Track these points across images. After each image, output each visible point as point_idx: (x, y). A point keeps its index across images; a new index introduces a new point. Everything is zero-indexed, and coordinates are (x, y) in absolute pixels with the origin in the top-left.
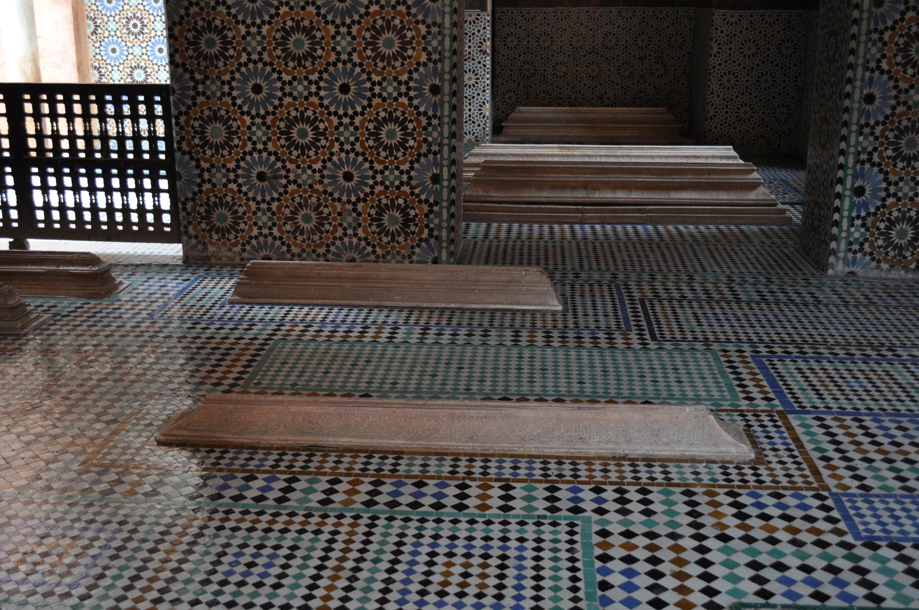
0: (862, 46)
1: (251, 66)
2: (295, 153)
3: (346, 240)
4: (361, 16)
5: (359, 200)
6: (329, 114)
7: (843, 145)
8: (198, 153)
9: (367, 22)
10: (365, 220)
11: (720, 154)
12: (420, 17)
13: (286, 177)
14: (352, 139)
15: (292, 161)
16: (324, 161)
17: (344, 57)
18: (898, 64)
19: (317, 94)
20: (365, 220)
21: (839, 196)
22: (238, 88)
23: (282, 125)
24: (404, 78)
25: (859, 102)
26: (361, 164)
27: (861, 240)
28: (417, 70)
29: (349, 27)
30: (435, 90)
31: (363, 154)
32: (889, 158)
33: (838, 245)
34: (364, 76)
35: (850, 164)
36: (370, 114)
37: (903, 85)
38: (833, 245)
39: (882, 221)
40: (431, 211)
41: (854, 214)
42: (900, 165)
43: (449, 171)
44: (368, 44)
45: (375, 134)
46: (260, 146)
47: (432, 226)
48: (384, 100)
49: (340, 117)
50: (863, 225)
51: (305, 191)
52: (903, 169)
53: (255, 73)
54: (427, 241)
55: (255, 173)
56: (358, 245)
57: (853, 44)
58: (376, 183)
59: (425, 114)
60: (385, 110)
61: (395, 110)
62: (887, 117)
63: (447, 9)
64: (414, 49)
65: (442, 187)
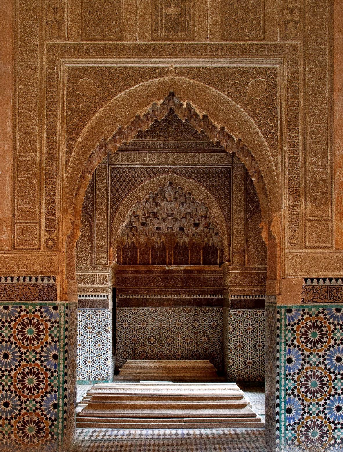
0: (283, 333)
3: (4, 441)
4: (16, 318)
5: (12, 418)
7: (278, 386)
9: (19, 320)
10: (15, 429)
12: (48, 318)
14: (9, 384)
17: (6, 339)
18: (303, 342)
20: (15, 429)
21: (278, 413)
25: (284, 362)
26: (14, 398)
27: (293, 438)
28: (45, 346)
29: (9, 323)
30: (55, 357)
31: (15, 392)
32: (303, 392)
33: (280, 441)
35: (283, 396)
36: (20, 370)
38: (278, 441)
39: (303, 427)
40: (53, 425)
41: (287, 423)
42: (309, 396)
43: (63, 402)
44: (19, 332)
45: (22, 381)
47: (53, 433)
48: (28, 362)
50: (293, 429)
52: (311, 398)
54: (50, 441)
56: (11, 444)
57: (278, 332)
58: (22, 408)
59: (50, 370)
60: (28, 368)
61: (33, 368)
62: (300, 370)
63: (62, 314)
64: (44, 335)
65: (59, 411)
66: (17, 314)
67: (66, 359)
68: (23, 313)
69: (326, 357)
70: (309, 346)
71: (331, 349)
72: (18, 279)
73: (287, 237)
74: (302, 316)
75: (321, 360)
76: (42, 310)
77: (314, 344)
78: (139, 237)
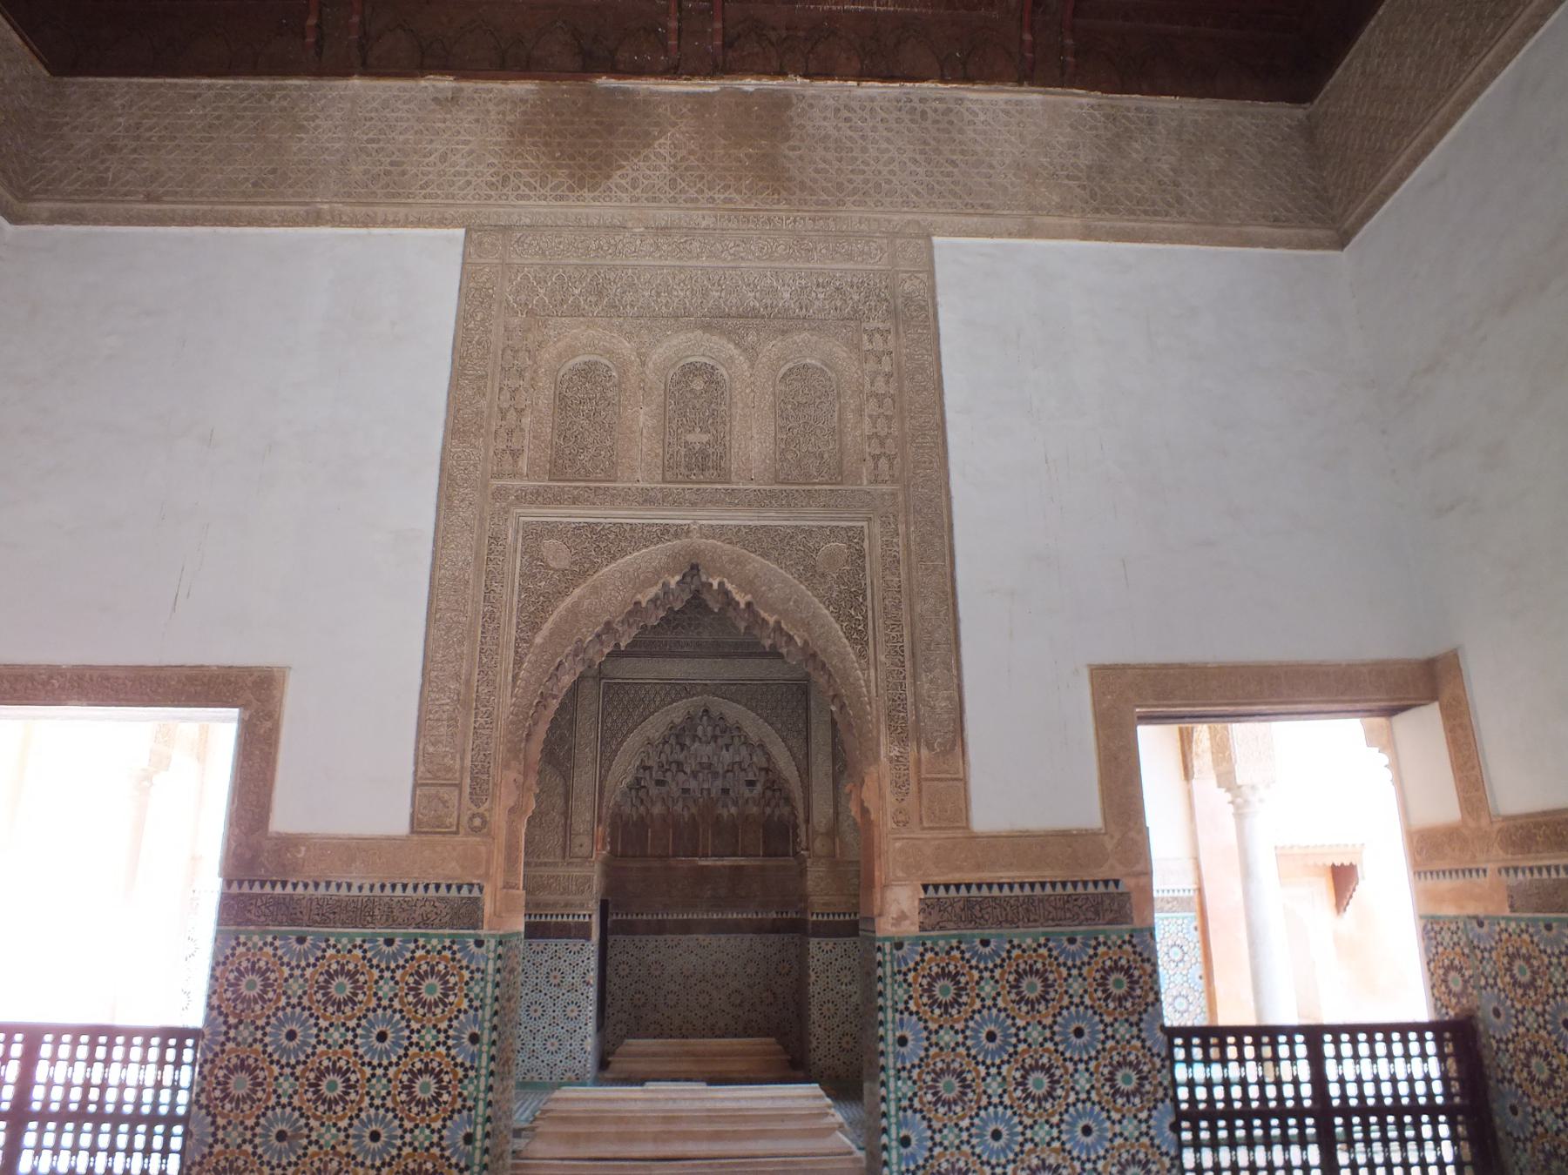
0: (889, 988)
1: (289, 1010)
2: (321, 1108)
6: (363, 1064)
7: (883, 1091)
8: (216, 1107)
11: (803, 1096)
12: (464, 963)
13: (308, 1137)
15: (316, 1118)
16: (351, 1118)
17: (385, 1002)
19: (352, 1042)
21: (885, 1148)
22: (271, 1034)
23: (312, 1076)
24: (444, 1025)
29: (393, 971)
30: (474, 1039)
34: (404, 1023)
35: (893, 1112)
36: (406, 1064)
37: (933, 1026)
44: (411, 989)
45: (408, 1088)
46: (284, 1100)
48: (421, 1049)
49: (374, 1068)
51: (326, 1154)
53: (292, 1018)
55: (275, 1131)
57: (880, 986)
59: (462, 1065)
63: (492, 955)
66: (408, 955)
67: (494, 1043)
68: (419, 953)
69: (968, 1033)
70: (937, 1011)
71: (977, 1016)
72: (415, 887)
73: (890, 810)
74: (922, 955)
75: (960, 1038)
76: (455, 947)
77: (946, 1007)
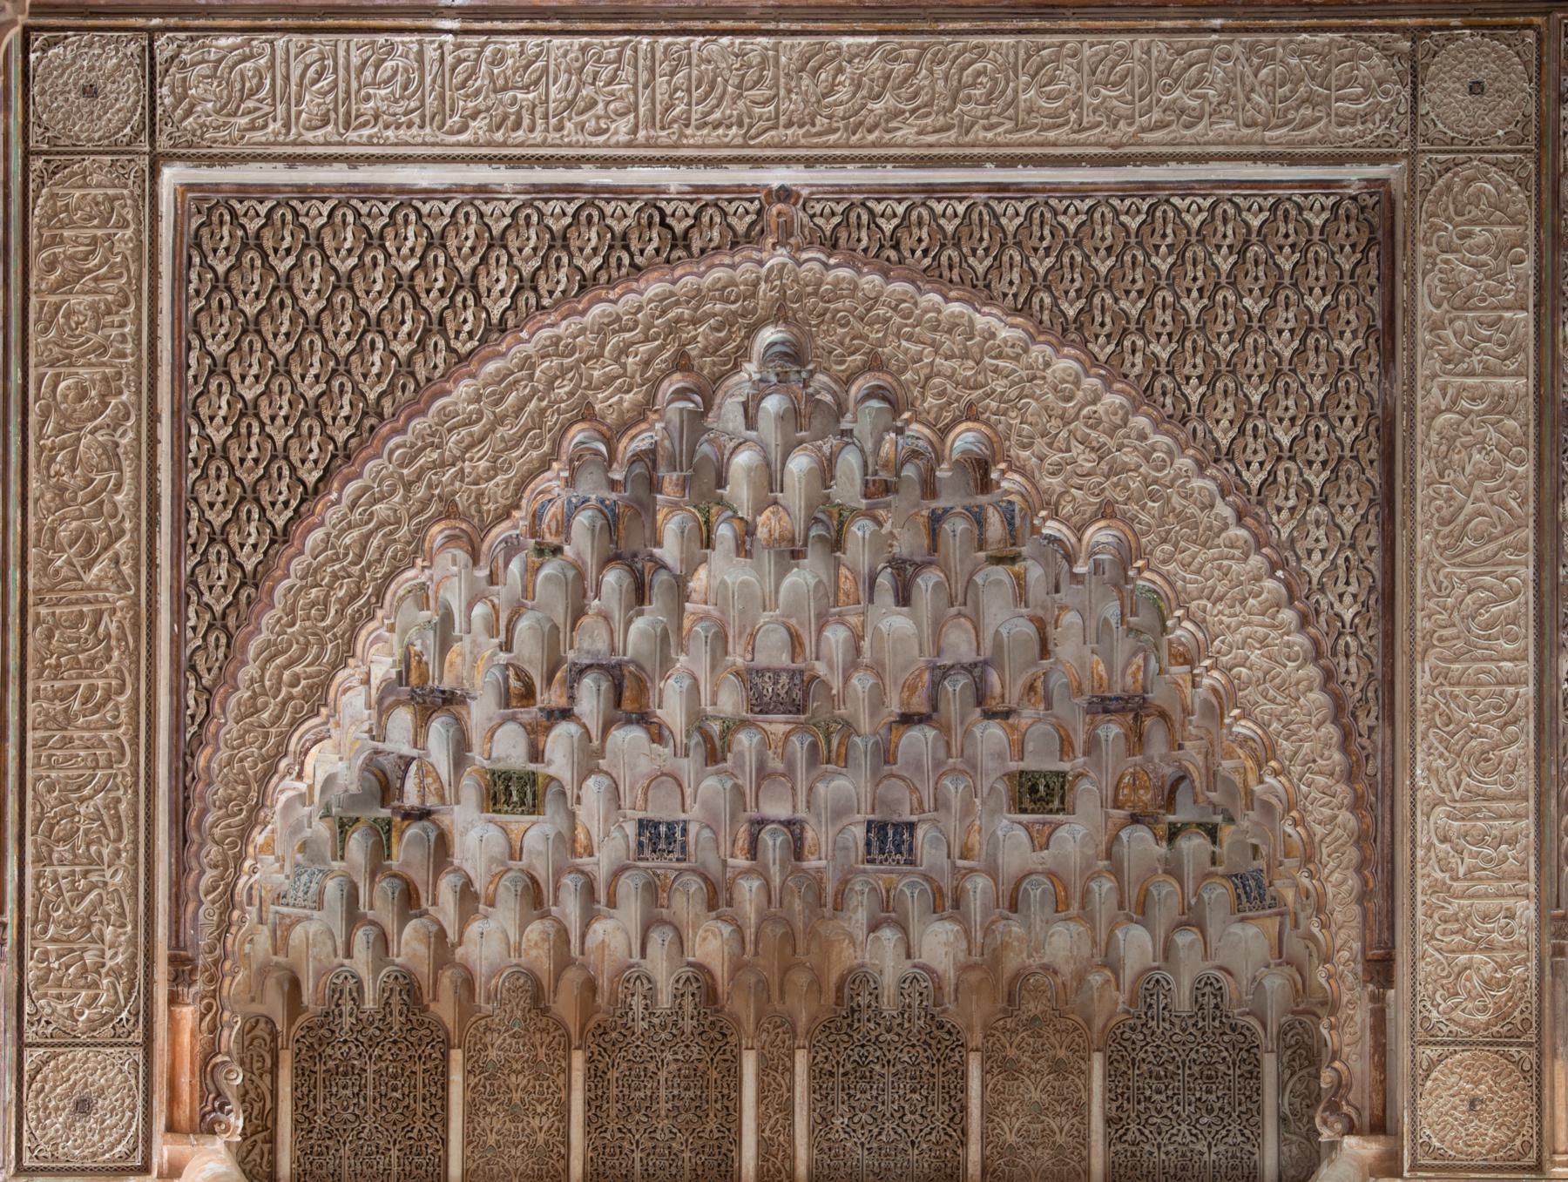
78: (464, 922)
